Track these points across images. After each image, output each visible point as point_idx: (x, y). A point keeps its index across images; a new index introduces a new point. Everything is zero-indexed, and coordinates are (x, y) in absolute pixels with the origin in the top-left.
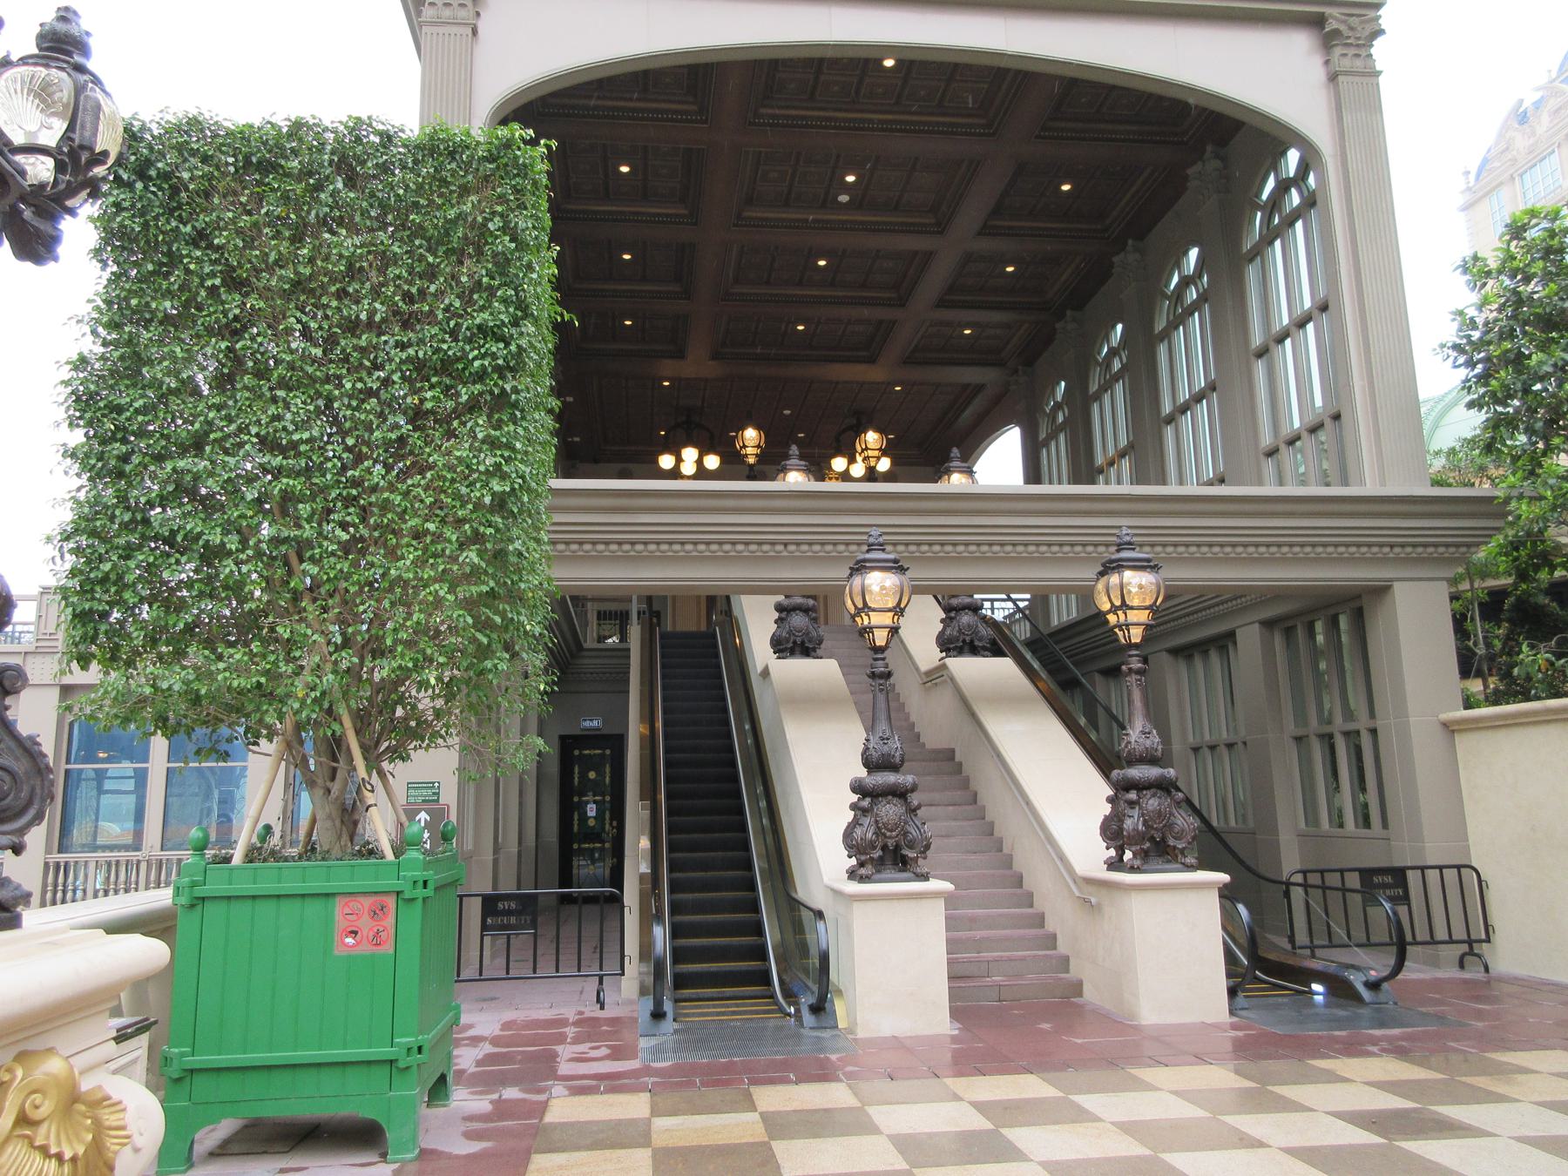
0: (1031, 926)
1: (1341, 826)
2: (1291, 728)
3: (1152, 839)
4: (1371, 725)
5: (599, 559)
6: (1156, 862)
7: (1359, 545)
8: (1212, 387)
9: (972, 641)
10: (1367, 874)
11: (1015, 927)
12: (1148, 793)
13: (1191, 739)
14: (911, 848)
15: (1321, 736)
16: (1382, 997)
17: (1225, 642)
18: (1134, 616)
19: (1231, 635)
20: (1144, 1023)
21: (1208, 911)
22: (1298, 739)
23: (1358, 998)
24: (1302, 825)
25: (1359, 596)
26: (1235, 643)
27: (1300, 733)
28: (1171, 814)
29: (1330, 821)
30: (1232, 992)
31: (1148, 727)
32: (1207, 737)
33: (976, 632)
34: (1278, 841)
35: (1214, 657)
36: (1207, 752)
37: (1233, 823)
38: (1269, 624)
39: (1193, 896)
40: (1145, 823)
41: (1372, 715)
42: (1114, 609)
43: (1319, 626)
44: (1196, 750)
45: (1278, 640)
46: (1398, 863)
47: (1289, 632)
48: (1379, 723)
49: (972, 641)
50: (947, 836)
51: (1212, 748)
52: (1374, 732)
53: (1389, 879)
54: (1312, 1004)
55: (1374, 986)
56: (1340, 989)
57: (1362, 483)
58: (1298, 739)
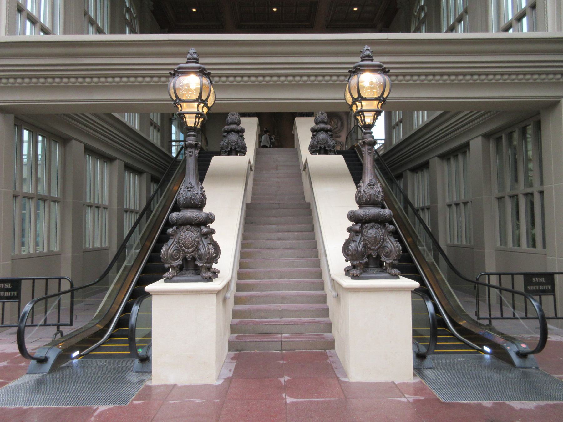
0: (319, 302)
1: (519, 246)
2: (496, 193)
3: (369, 257)
4: (540, 189)
5: (66, 88)
6: (373, 272)
7: (540, 74)
8: (466, 11)
9: (325, 148)
10: (528, 277)
11: (308, 302)
12: (369, 225)
13: (447, 201)
14: (200, 259)
15: (512, 197)
16: (528, 363)
17: (464, 148)
18: (366, 105)
19: (467, 145)
20: (352, 380)
21: (405, 305)
22: (499, 199)
23: (511, 362)
24: (498, 244)
25: (539, 113)
26: (469, 149)
27: (500, 195)
28: (384, 240)
29: (513, 243)
30: (420, 357)
31: (374, 181)
32: (455, 199)
33: (327, 143)
34: (484, 253)
35: (460, 158)
36: (454, 207)
37: (464, 243)
38: (487, 136)
39: (392, 297)
40: (365, 246)
41: (542, 183)
42: (355, 101)
43: (516, 135)
44: (450, 206)
45: (492, 145)
46: (550, 270)
47: (498, 140)
48: (545, 188)
49: (325, 148)
50: (291, 248)
51: (457, 204)
52: (542, 193)
53: (543, 280)
54: (482, 358)
55: (522, 355)
56: (500, 353)
57: (545, 29)
58: (499, 199)
